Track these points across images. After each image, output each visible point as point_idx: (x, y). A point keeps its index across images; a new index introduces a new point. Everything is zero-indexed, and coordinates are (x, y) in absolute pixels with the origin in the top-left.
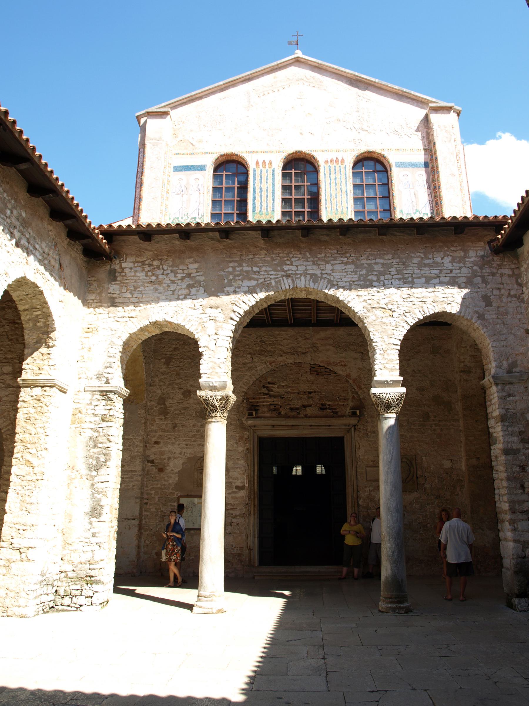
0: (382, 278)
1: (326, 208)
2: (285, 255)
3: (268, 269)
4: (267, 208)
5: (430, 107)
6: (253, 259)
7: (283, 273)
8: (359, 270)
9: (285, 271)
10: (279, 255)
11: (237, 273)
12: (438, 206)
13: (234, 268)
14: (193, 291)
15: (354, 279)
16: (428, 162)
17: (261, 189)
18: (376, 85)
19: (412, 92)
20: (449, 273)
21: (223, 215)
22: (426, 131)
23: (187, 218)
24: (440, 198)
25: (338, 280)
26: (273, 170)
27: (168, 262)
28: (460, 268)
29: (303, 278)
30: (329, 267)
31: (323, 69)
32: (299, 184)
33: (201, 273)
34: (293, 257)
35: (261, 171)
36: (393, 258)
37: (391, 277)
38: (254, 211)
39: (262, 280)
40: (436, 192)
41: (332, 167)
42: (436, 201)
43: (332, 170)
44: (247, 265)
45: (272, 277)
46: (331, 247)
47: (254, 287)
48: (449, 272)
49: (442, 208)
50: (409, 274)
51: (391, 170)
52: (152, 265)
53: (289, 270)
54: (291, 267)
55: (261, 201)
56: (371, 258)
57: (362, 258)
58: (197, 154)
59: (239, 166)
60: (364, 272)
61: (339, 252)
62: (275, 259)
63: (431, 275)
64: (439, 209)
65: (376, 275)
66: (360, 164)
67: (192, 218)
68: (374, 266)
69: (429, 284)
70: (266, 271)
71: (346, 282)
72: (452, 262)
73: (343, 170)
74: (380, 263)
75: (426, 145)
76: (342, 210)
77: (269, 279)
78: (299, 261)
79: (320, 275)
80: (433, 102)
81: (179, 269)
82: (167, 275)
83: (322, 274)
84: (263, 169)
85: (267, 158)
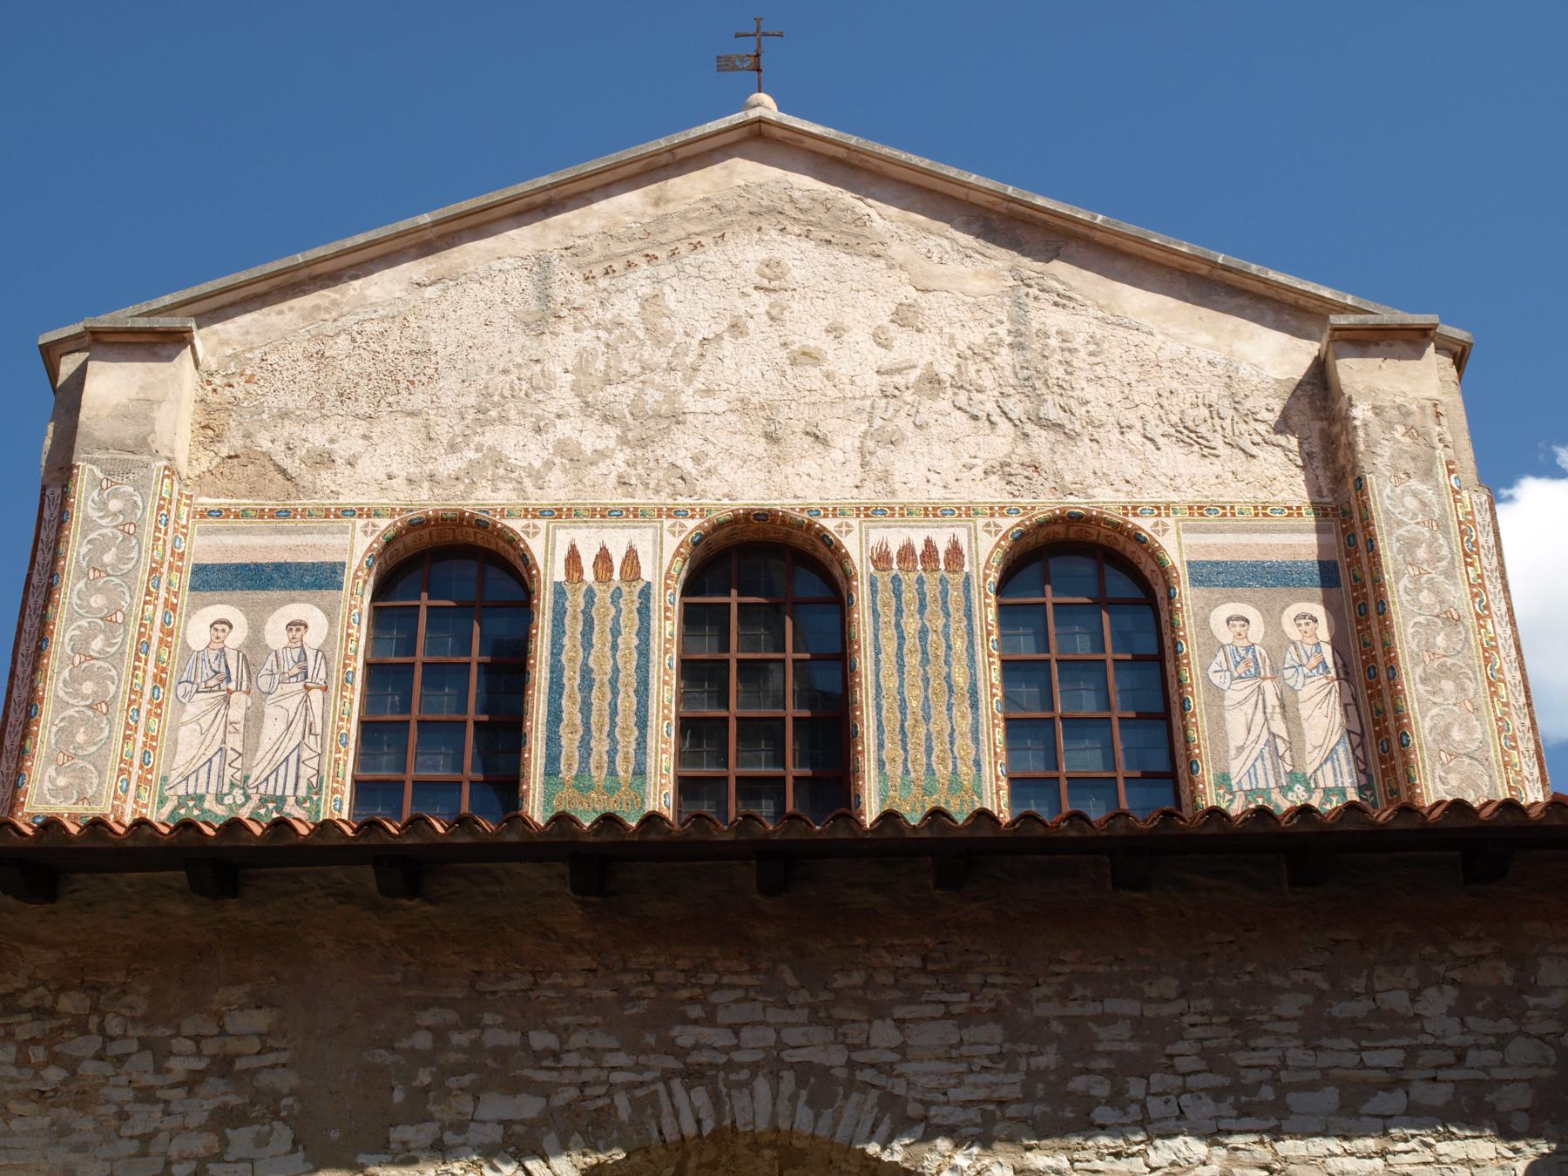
0: (1136, 1088)
1: (881, 764)
2: (681, 978)
3: (601, 1040)
4: (612, 762)
5: (1336, 329)
6: (533, 995)
7: (671, 1063)
8: (1023, 1048)
9: (681, 1053)
10: (651, 974)
11: (454, 1057)
12: (1392, 758)
13: (439, 1033)
14: (241, 1138)
15: (1003, 1093)
16: (1335, 564)
17: (586, 674)
18: (1098, 236)
19: (1254, 268)
20: (1449, 1066)
21: (409, 788)
22: (1322, 430)
23: (240, 799)
24: (1398, 719)
25: (929, 1097)
26: (645, 593)
27: (128, 999)
28: (1502, 1041)
29: (762, 1086)
30: (884, 1034)
31: (869, 172)
32: (759, 656)
33: (284, 1057)
34: (717, 986)
35: (590, 595)
36: (1182, 995)
37: (1179, 1081)
38: (552, 769)
39: (572, 1093)
40: (1380, 693)
42: (1378, 735)
43: (909, 595)
44: (500, 1019)
45: (616, 1077)
46: (896, 941)
47: (530, 1124)
48: (1449, 1057)
49: (1407, 764)
50: (1262, 1067)
51: (1170, 598)
52: (52, 1013)
53: (697, 1047)
54: (708, 1034)
56: (1079, 991)
57: (1037, 993)
58: (307, 514)
59: (492, 573)
60: (1048, 1059)
61: (930, 967)
62: (633, 992)
63: (1364, 1073)
64: (1393, 769)
65: (1106, 1072)
66: (1034, 570)
67: (264, 801)
68: (1095, 1029)
69: (1357, 1114)
70: (591, 1050)
71: (966, 1104)
72: (1459, 1011)
73: (955, 595)
74: (1124, 1017)
75: (1325, 492)
76: (954, 772)
77: (602, 1090)
78: (747, 1006)
79: (841, 1074)
80: (1344, 309)
81: (177, 1035)
82: (121, 1060)
83: (851, 1065)
84: (595, 587)
85: (617, 541)
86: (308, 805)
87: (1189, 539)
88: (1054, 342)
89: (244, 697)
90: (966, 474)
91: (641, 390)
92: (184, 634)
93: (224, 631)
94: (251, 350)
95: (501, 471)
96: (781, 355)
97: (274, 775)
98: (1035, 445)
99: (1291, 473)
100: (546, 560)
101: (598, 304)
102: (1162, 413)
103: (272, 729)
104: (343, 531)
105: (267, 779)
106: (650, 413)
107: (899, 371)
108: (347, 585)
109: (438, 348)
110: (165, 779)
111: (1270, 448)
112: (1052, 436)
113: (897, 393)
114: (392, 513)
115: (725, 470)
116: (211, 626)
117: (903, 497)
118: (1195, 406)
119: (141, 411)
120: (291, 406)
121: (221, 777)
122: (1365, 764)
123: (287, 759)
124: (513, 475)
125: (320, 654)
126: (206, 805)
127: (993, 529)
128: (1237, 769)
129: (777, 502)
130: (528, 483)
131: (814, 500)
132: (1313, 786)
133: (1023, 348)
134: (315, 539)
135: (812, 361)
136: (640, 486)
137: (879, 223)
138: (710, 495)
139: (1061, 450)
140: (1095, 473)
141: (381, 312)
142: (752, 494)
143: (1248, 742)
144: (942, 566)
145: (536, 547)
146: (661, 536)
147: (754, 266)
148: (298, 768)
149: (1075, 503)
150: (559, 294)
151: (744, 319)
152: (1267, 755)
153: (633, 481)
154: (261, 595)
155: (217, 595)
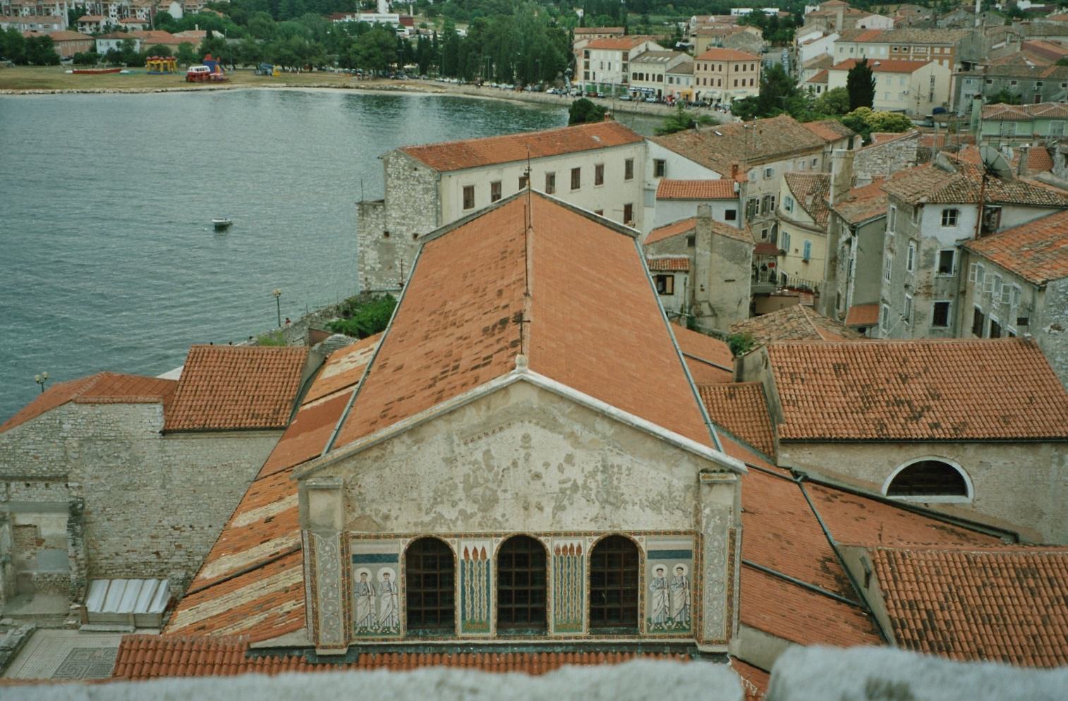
17: (472, 588)
26: (488, 563)
35: (472, 563)
41: (565, 560)
58: (385, 537)
87: (649, 543)
88: (616, 470)
91: (484, 492)
96: (528, 475)
103: (384, 607)
114: (410, 536)
115: (511, 521)
117: (565, 529)
119: (330, 511)
128: (653, 616)
131: (538, 530)
134: (389, 546)
137: (561, 420)
145: (455, 547)
147: (520, 437)
149: (617, 530)
150: (457, 450)
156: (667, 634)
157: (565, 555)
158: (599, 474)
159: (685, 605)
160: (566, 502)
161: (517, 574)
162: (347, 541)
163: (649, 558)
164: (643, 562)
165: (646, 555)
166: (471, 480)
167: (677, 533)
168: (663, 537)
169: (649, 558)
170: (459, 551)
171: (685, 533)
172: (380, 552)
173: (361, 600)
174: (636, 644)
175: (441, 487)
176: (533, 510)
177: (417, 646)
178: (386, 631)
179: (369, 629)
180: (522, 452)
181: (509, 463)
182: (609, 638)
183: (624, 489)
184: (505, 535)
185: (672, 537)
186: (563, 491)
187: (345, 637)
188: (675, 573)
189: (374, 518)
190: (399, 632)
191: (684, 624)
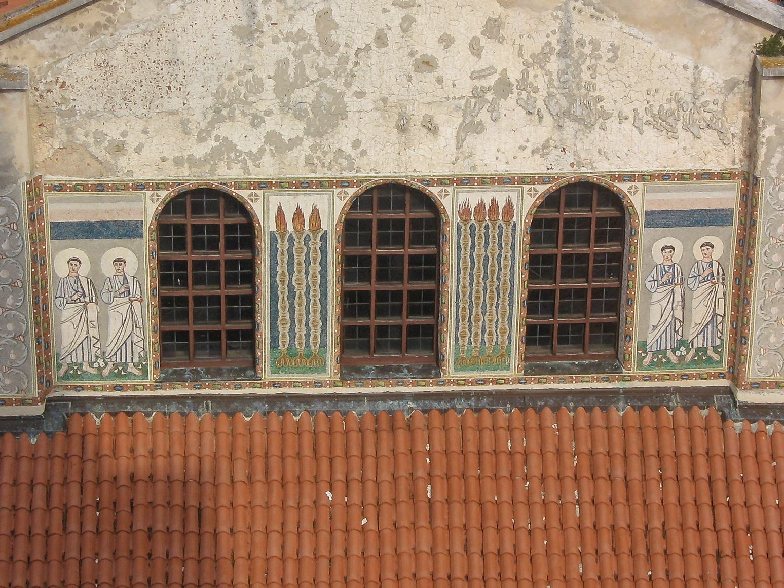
26: (324, 238)
35: (291, 239)
38: (274, 344)
41: (480, 231)
55: (293, 322)
58: (115, 187)
75: (737, 160)
84: (294, 235)
85: (306, 202)
86: (140, 367)
87: (648, 196)
88: (587, 50)
89: (95, 305)
90: (520, 154)
91: (318, 95)
92: (54, 270)
93: (76, 265)
94: (59, 61)
95: (232, 155)
97: (120, 351)
98: (564, 132)
99: (719, 148)
100: (264, 218)
101: (287, 19)
102: (648, 106)
104: (139, 199)
105: (116, 354)
106: (325, 112)
107: (485, 76)
108: (146, 234)
109: (183, 58)
110: (58, 354)
111: (710, 131)
112: (576, 126)
113: (481, 94)
114: (167, 186)
116: (68, 262)
117: (481, 171)
118: (669, 101)
120: (93, 109)
121: (89, 353)
122: (722, 334)
123: (125, 342)
124: (240, 158)
125: (135, 279)
126: (84, 368)
127: (533, 192)
128: (651, 338)
129: (404, 174)
130: (250, 163)
131: (424, 171)
132: (690, 347)
133: (566, 57)
134: (123, 205)
135: (428, 68)
136: (319, 164)
138: (362, 170)
139: (581, 137)
140: (599, 152)
141: (142, 27)
142: (389, 169)
143: (661, 323)
144: (500, 218)
146: (333, 200)
148: (132, 347)
151: (385, 32)
152: (669, 328)
153: (315, 161)
154: (96, 242)
155: (69, 242)
156: (675, 372)
157: (480, 222)
158: (554, 58)
159: (715, 315)
160: (484, 116)
161: (382, 259)
162: (39, 196)
163: (647, 225)
164: (634, 234)
165: (642, 219)
166: (291, 72)
167: (705, 176)
168: (676, 183)
169: (647, 225)
170: (265, 211)
171: (721, 176)
172: (107, 218)
173: (69, 311)
174: (615, 393)
175: (228, 86)
176: (417, 131)
177: (181, 399)
178: (120, 371)
179: (86, 367)
180: (397, 15)
181: (370, 38)
182: (564, 381)
183: (602, 89)
184: (360, 182)
185: (696, 183)
186: (478, 94)
187: (40, 383)
188: (698, 254)
189: (93, 149)
190: (145, 371)
191: (710, 352)
